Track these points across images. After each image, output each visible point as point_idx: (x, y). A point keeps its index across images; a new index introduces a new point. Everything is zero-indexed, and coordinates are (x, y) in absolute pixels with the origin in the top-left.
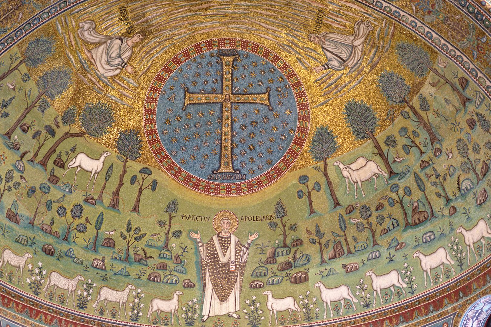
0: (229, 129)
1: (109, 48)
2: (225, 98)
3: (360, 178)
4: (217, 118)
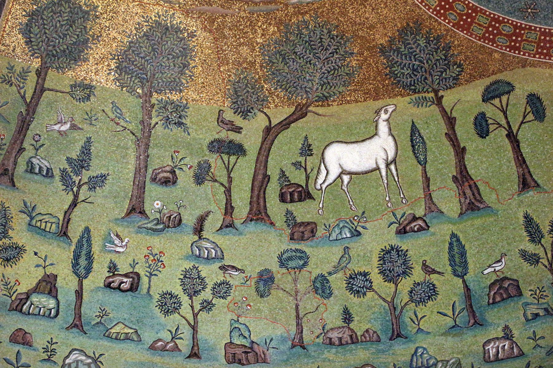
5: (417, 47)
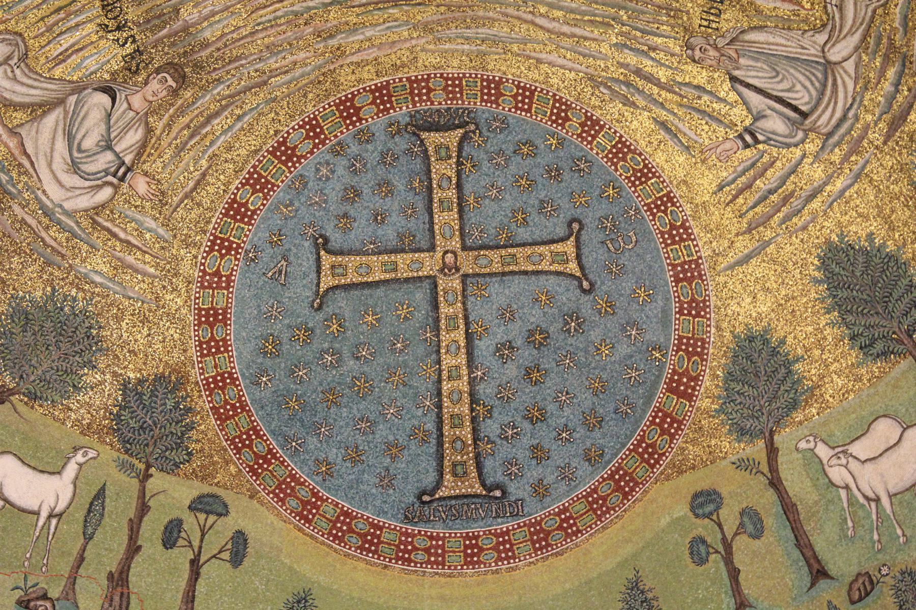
0: (462, 359)
2: (444, 263)
3: (885, 483)
4: (421, 328)
5: (162, 405)
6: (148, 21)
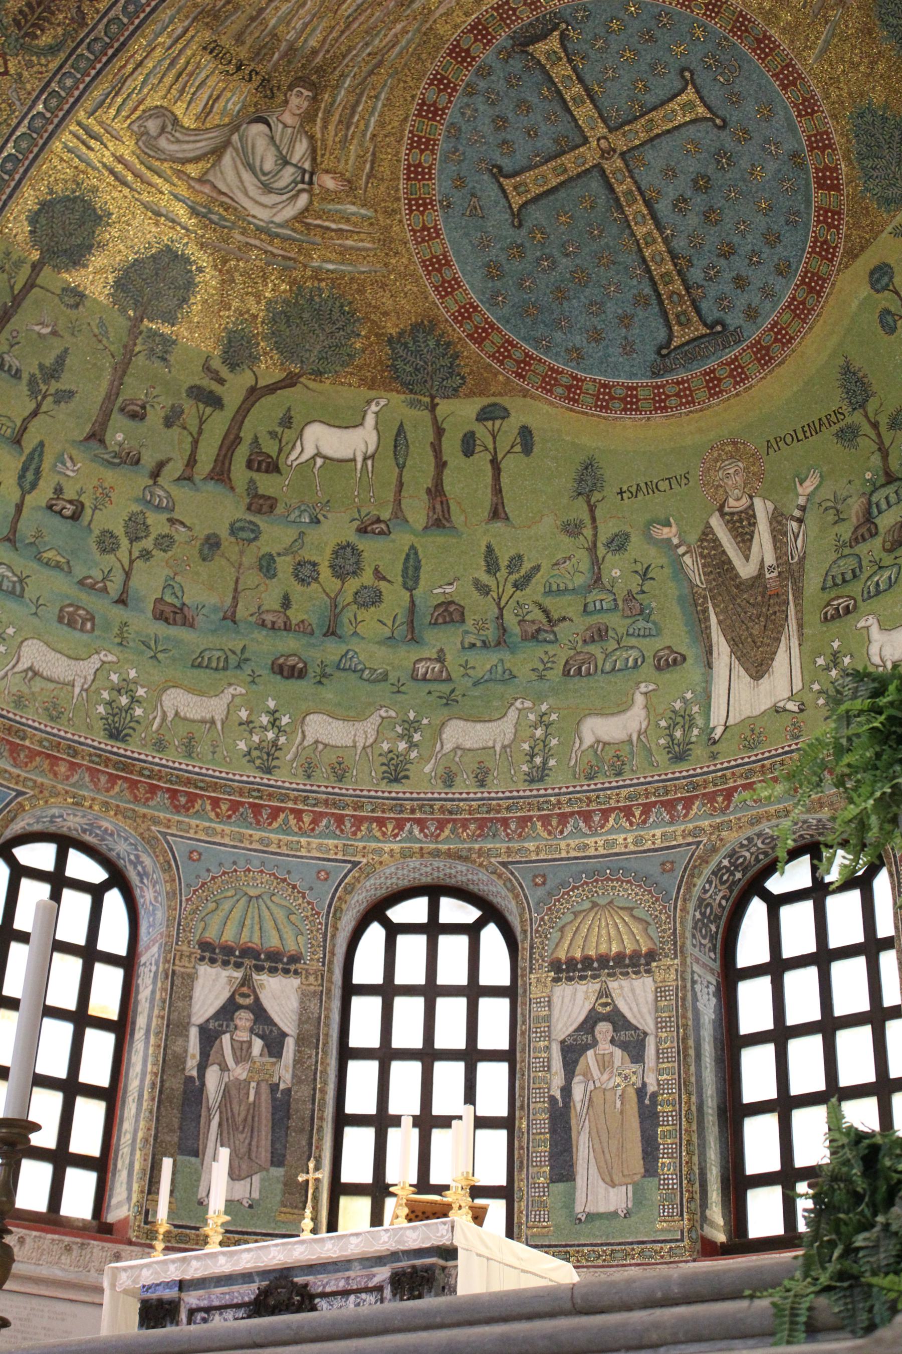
0: (650, 225)
1: (245, 154)
2: (601, 149)
4: (607, 211)
6: (258, 54)
